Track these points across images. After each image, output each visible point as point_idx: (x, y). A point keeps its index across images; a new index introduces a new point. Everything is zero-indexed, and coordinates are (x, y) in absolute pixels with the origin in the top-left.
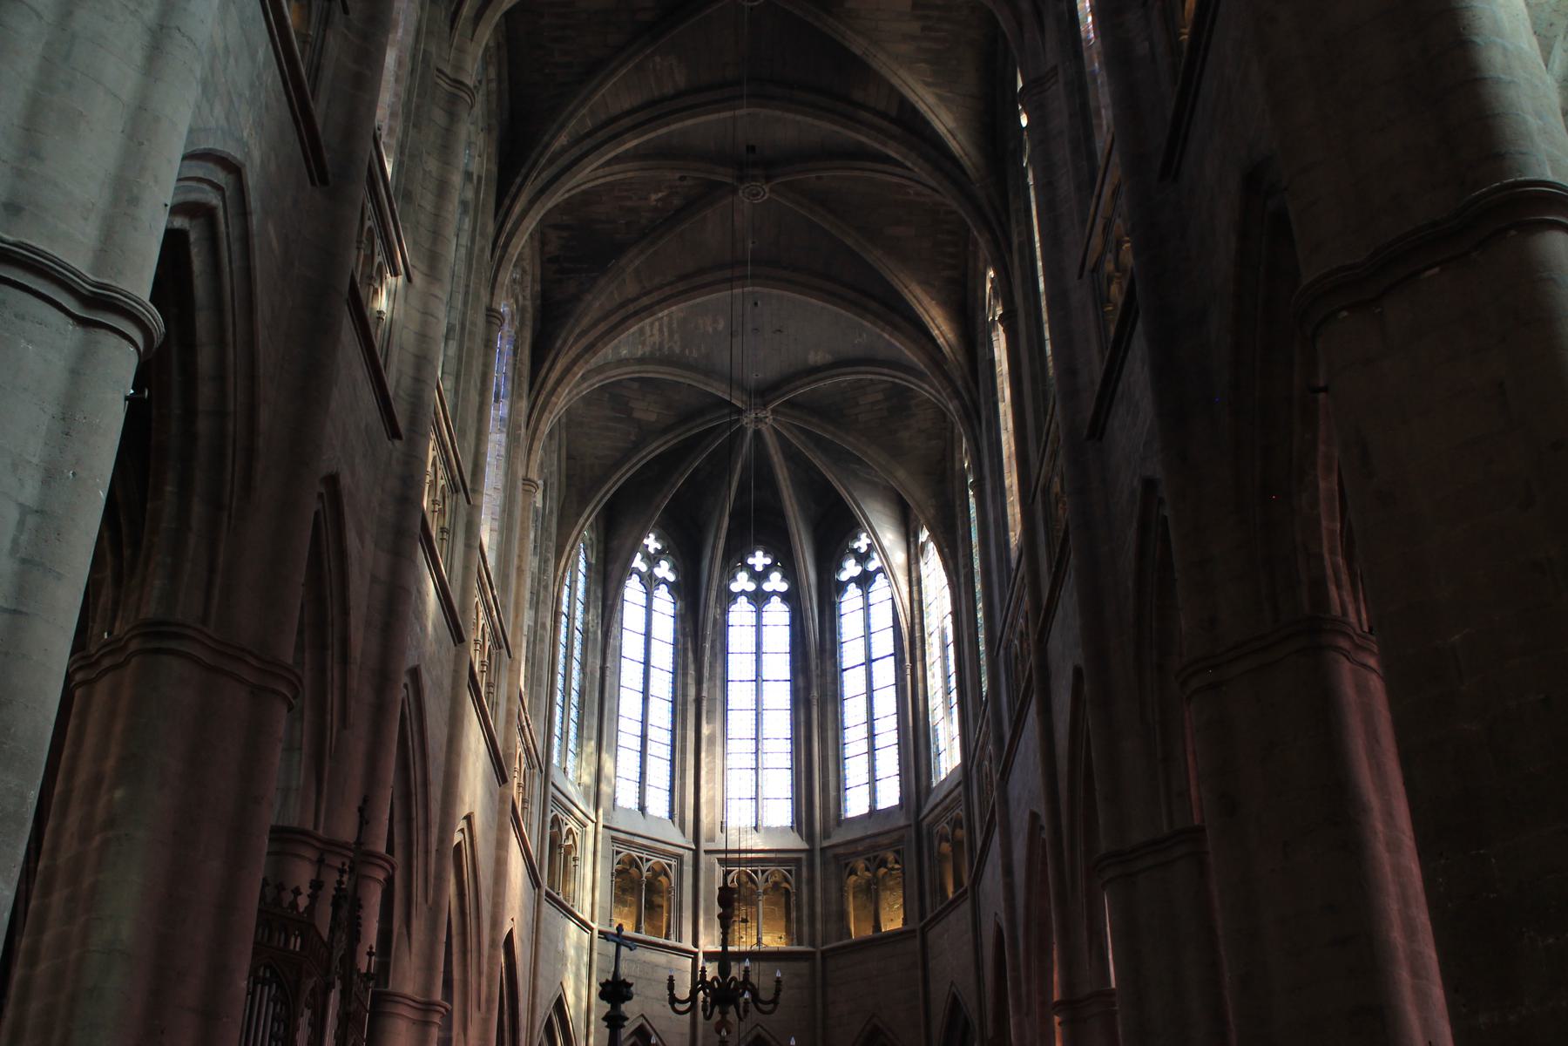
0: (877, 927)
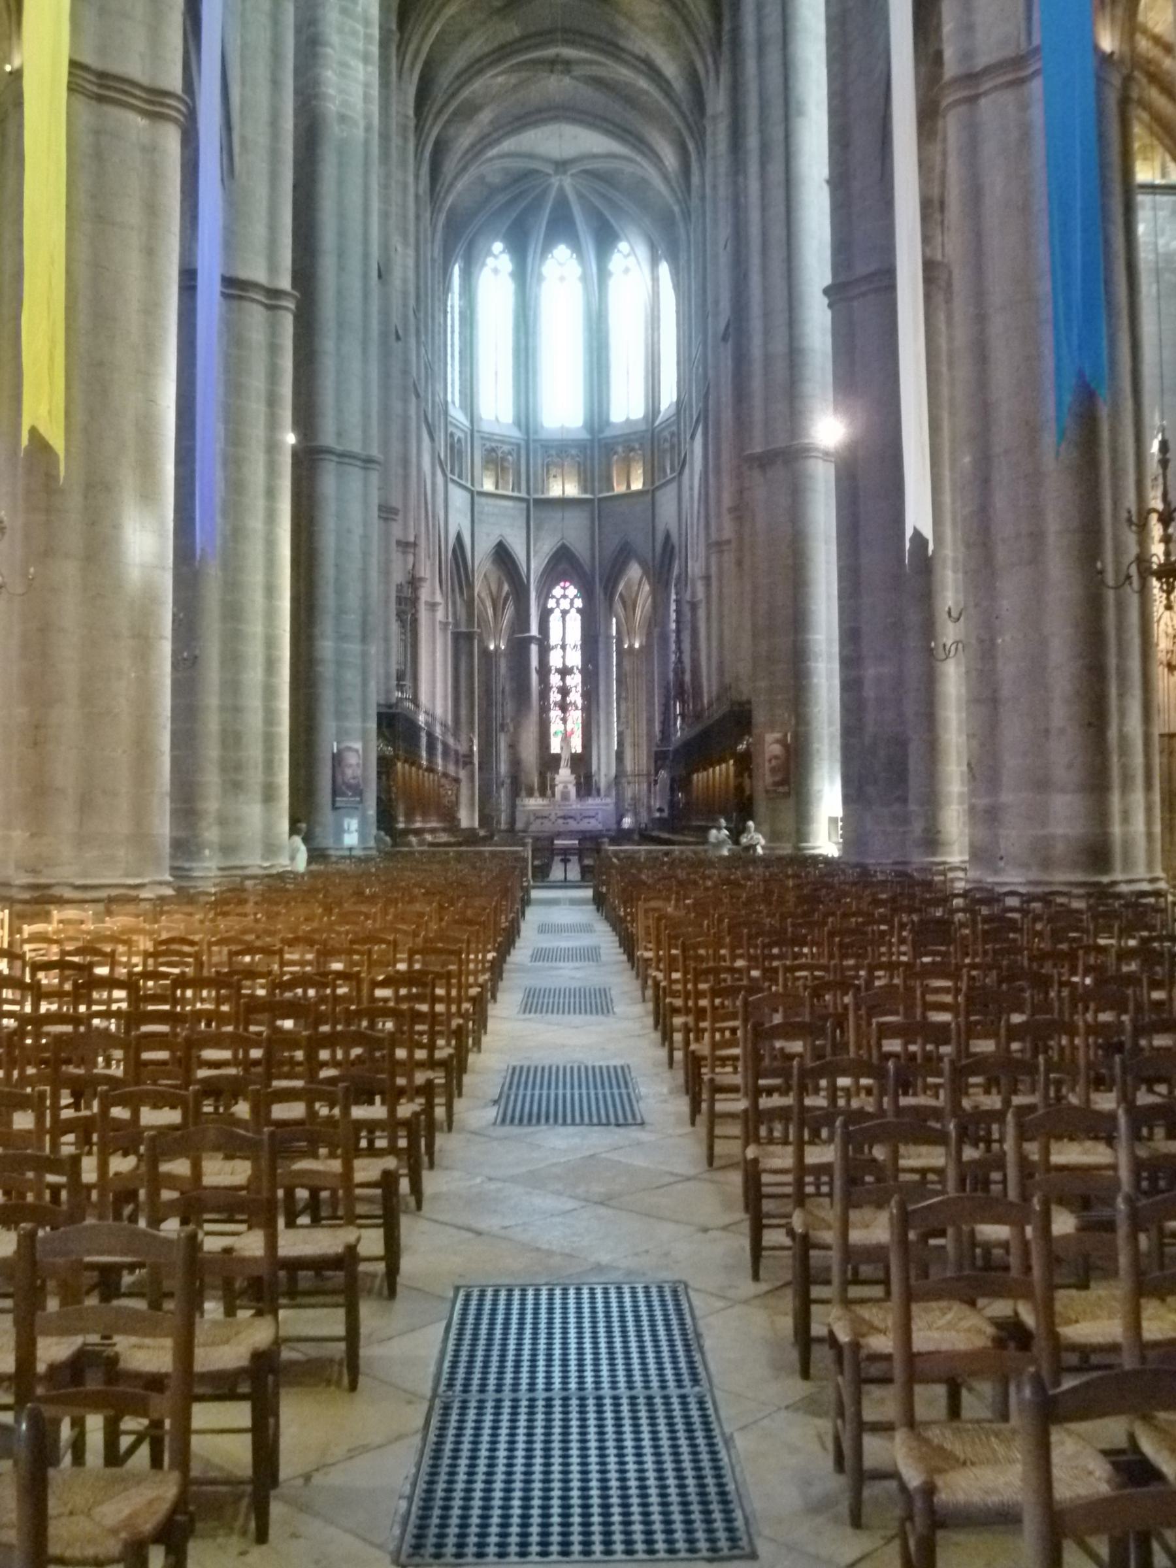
0: (629, 486)
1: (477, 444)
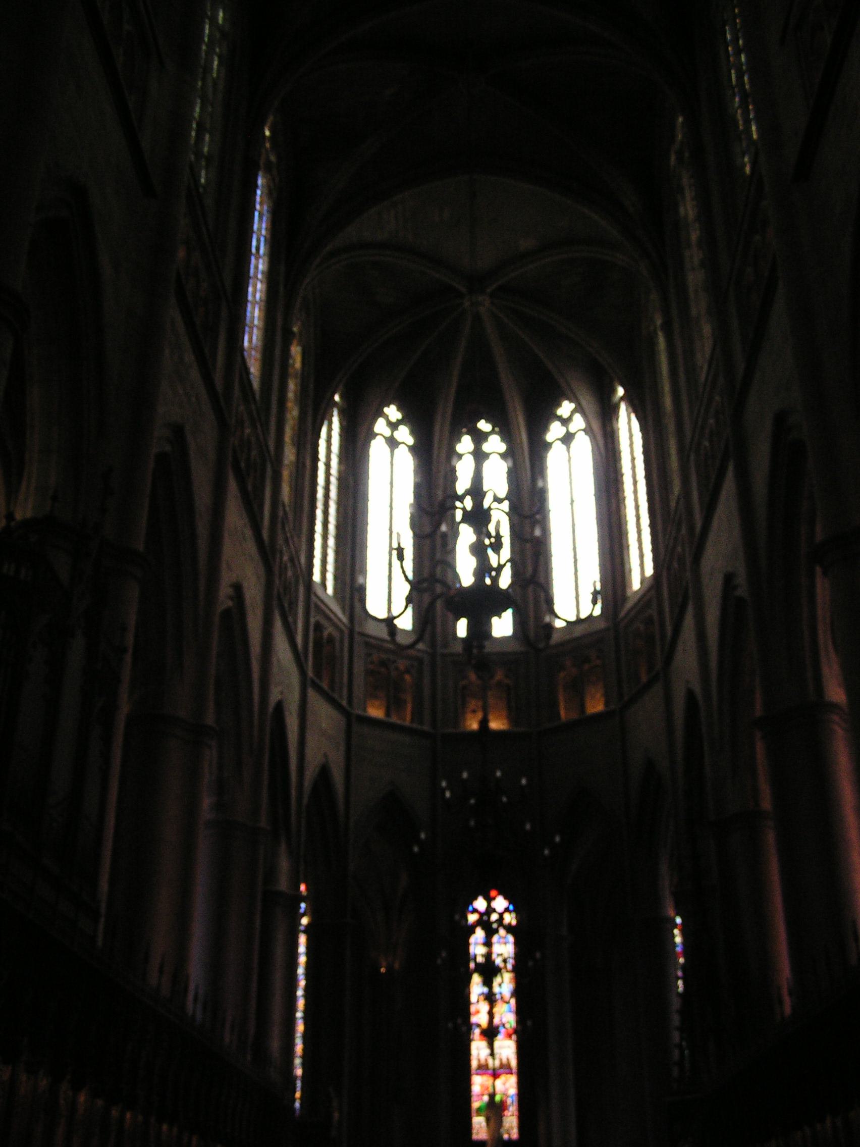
1: (359, 650)
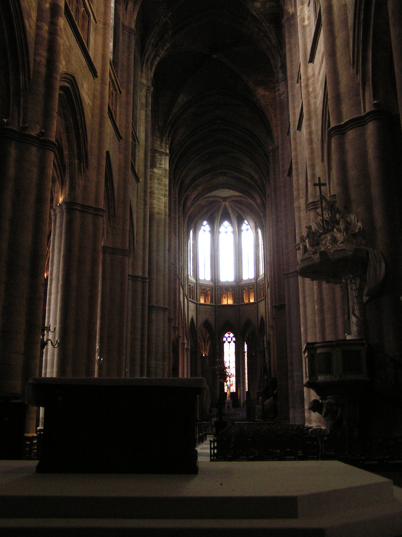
0: (249, 301)
1: (198, 287)
